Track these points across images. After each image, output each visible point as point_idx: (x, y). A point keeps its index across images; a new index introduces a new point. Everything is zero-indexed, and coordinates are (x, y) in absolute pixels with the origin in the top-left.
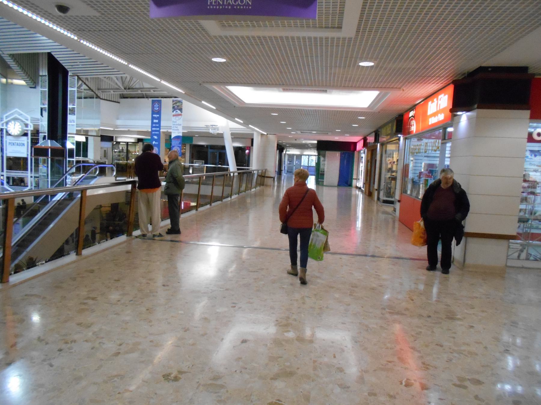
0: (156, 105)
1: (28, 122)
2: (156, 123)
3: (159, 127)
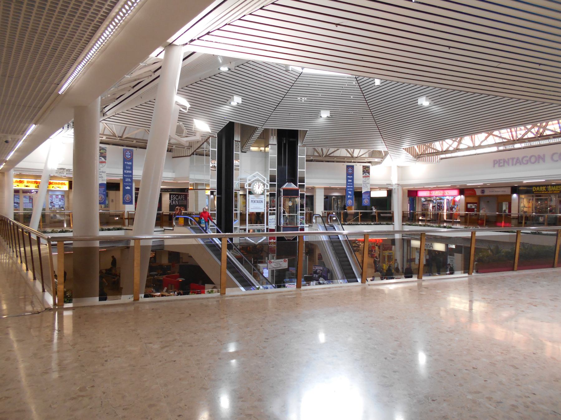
0: (350, 169)
1: (265, 182)
2: (350, 182)
3: (353, 185)
